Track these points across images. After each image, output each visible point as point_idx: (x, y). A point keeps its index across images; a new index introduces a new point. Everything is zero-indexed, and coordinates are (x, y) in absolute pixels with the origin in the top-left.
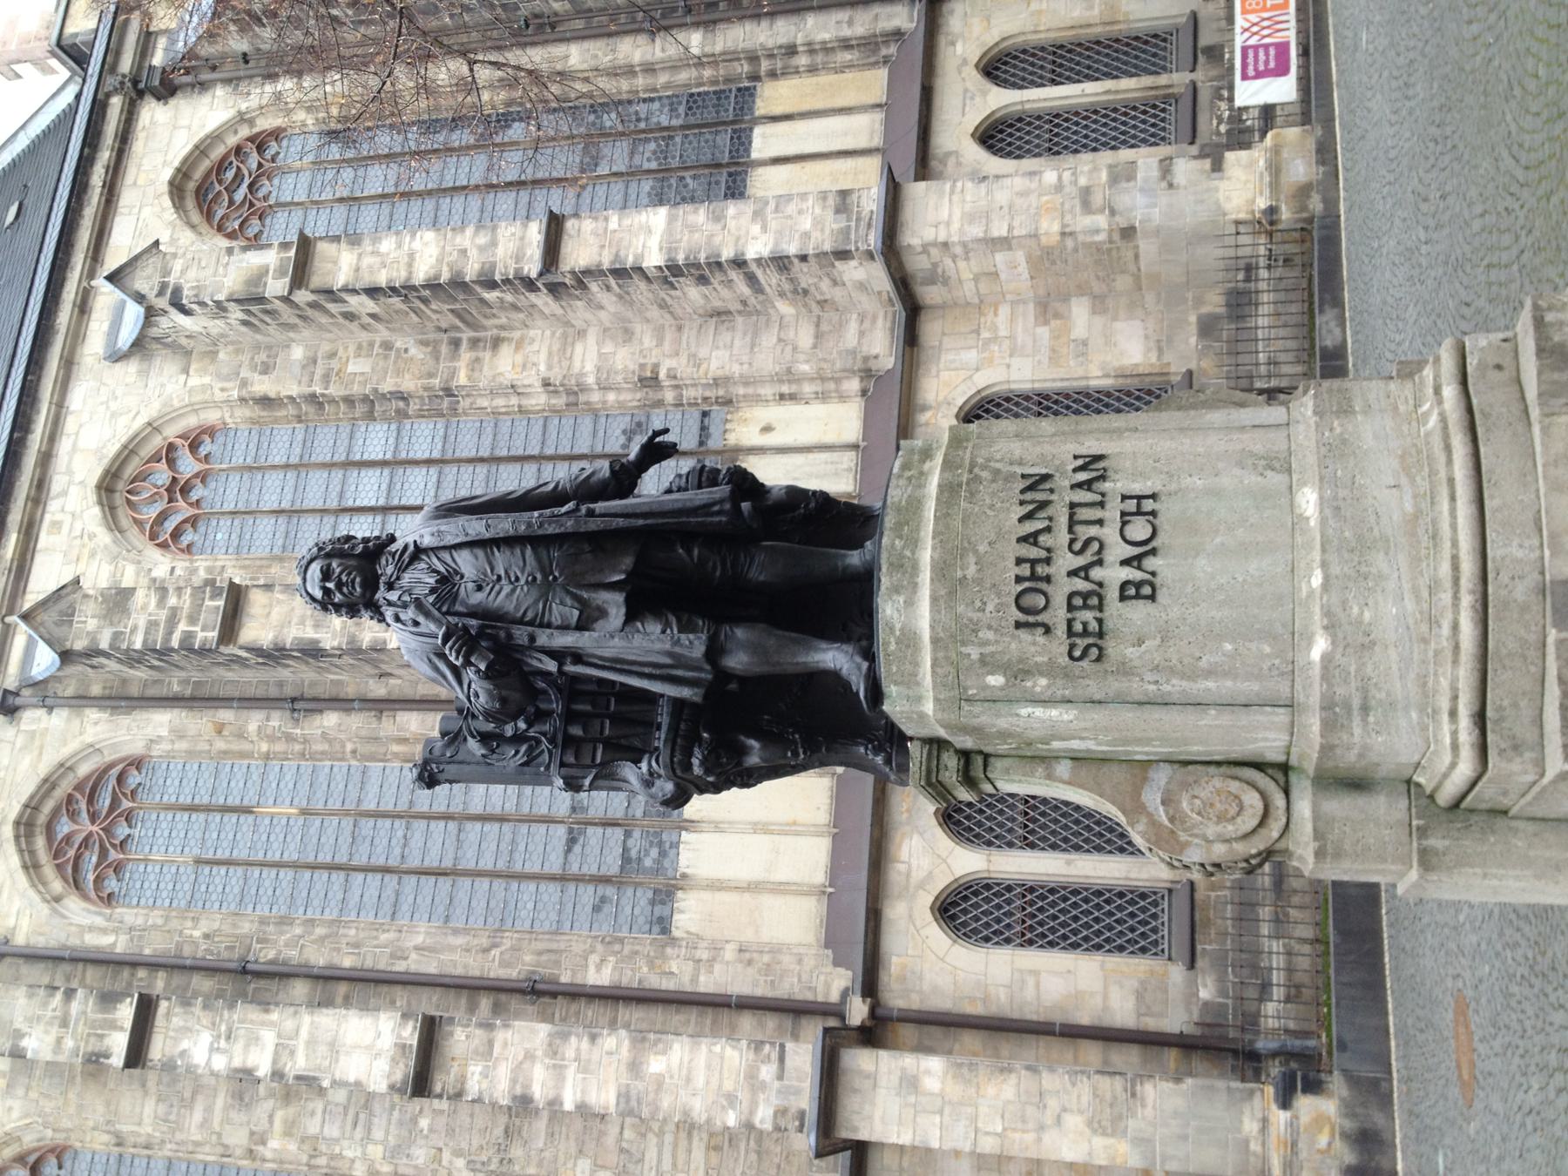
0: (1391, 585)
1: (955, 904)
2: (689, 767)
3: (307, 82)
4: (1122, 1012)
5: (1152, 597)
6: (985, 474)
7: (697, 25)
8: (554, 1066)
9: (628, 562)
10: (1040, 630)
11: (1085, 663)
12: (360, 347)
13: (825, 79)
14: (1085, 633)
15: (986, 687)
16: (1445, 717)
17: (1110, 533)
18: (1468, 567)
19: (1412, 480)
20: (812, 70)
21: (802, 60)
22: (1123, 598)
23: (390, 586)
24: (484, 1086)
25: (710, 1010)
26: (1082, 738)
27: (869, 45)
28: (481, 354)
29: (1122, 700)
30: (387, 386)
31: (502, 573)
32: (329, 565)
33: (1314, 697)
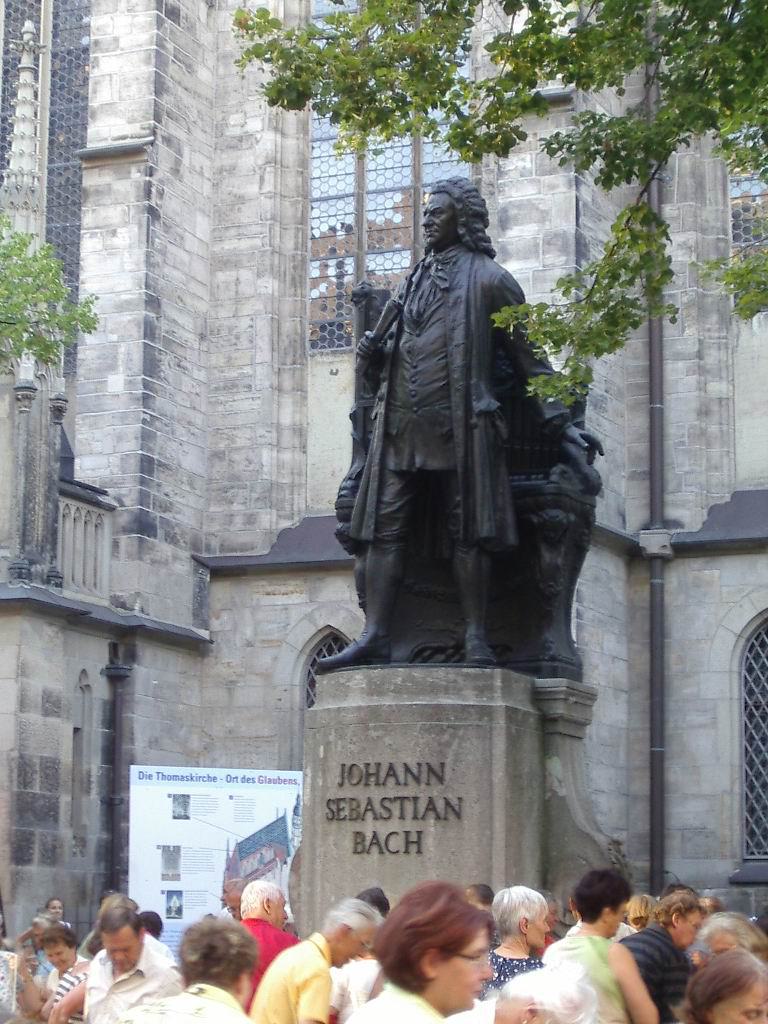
4: (683, 813)
5: (355, 852)
6: (446, 737)
8: (538, 244)
9: (435, 464)
17: (394, 825)
22: (359, 834)
24: (514, 175)
25: (647, 380)
31: (419, 369)
32: (442, 212)
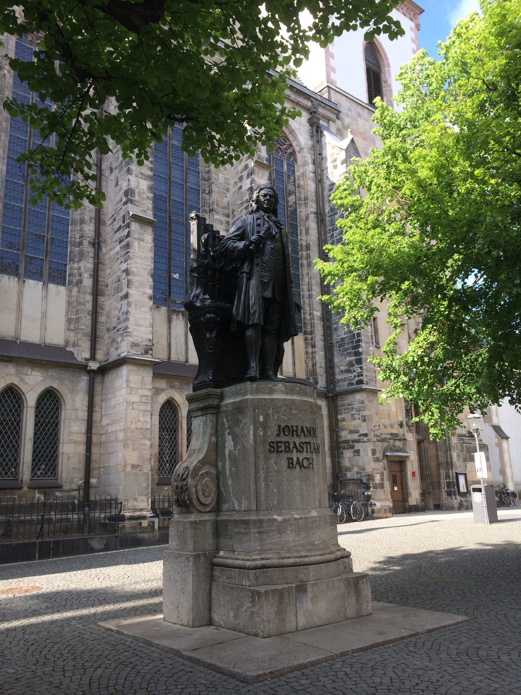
0: (297, 538)
1: (12, 392)
2: (210, 313)
3: (312, 175)
5: (289, 467)
7: (323, 314)
10: (278, 433)
11: (268, 447)
12: (228, 180)
13: (303, 357)
14: (278, 447)
15: (259, 416)
16: (260, 557)
17: (304, 455)
18: (306, 560)
19: (321, 543)
20: (307, 353)
21: (310, 350)
23: (268, 217)
26: (235, 446)
27: (313, 373)
28: (224, 225)
29: (257, 458)
30: (214, 187)
33: (262, 517)
